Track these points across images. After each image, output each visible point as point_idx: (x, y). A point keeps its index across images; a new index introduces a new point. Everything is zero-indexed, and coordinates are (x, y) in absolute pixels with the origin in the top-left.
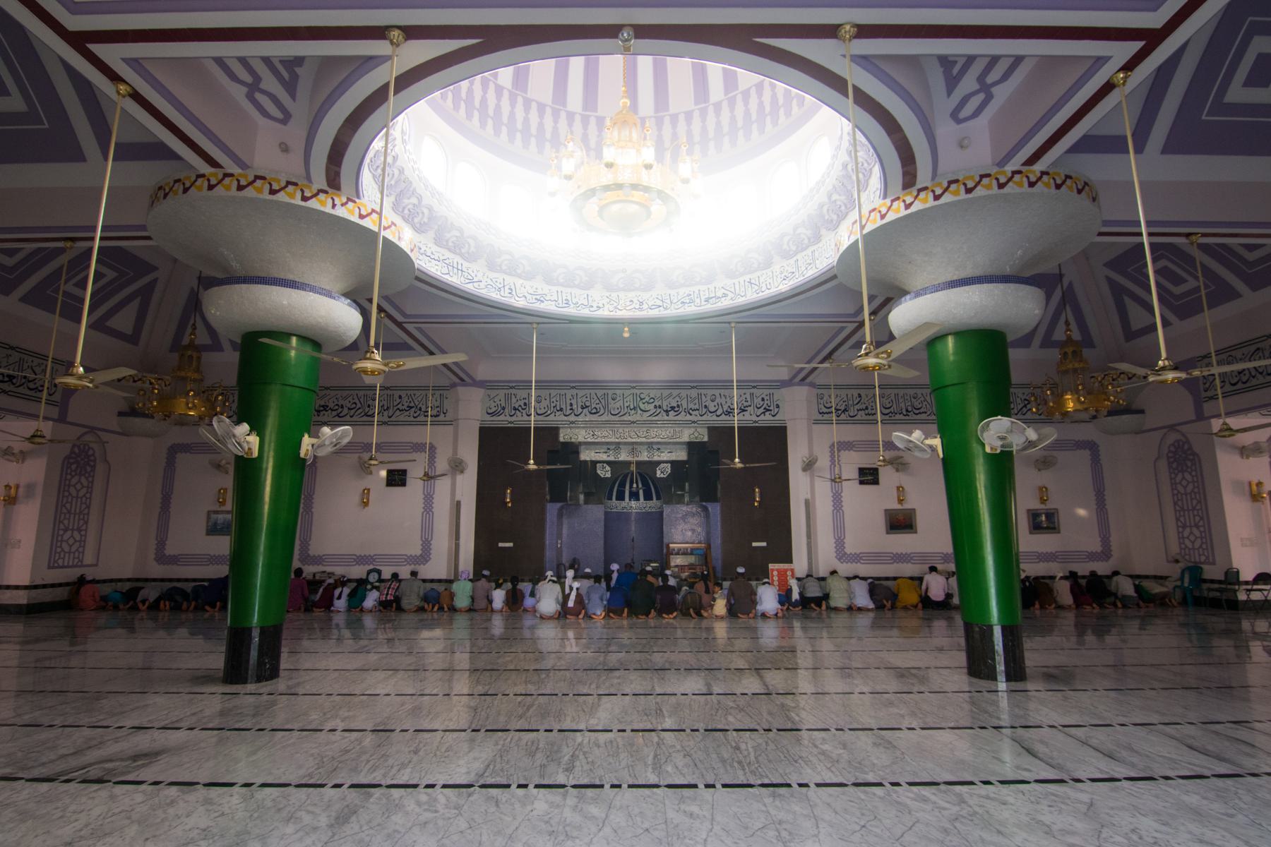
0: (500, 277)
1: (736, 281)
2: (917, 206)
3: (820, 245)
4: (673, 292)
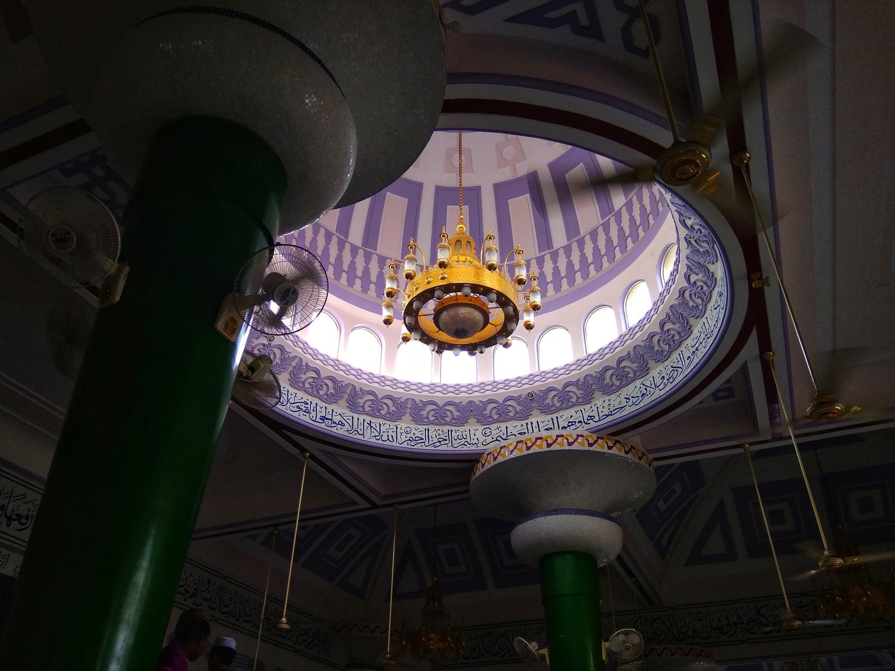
1: (356, 416)
2: (614, 451)
3: (461, 429)
4: (292, 390)
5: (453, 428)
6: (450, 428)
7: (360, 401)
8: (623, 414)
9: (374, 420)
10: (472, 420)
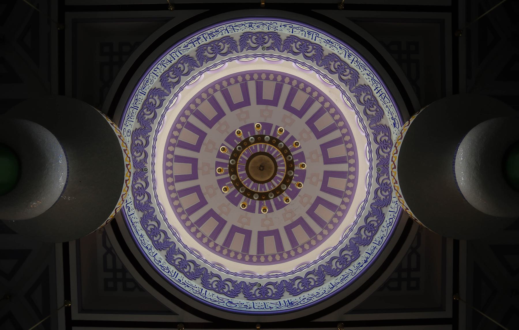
0: (353, 65)
1: (180, 56)
3: (136, 116)
4: (227, 34)
5: (138, 111)
6: (139, 109)
7: (187, 64)
8: (135, 233)
9: (171, 64)
10: (138, 126)
